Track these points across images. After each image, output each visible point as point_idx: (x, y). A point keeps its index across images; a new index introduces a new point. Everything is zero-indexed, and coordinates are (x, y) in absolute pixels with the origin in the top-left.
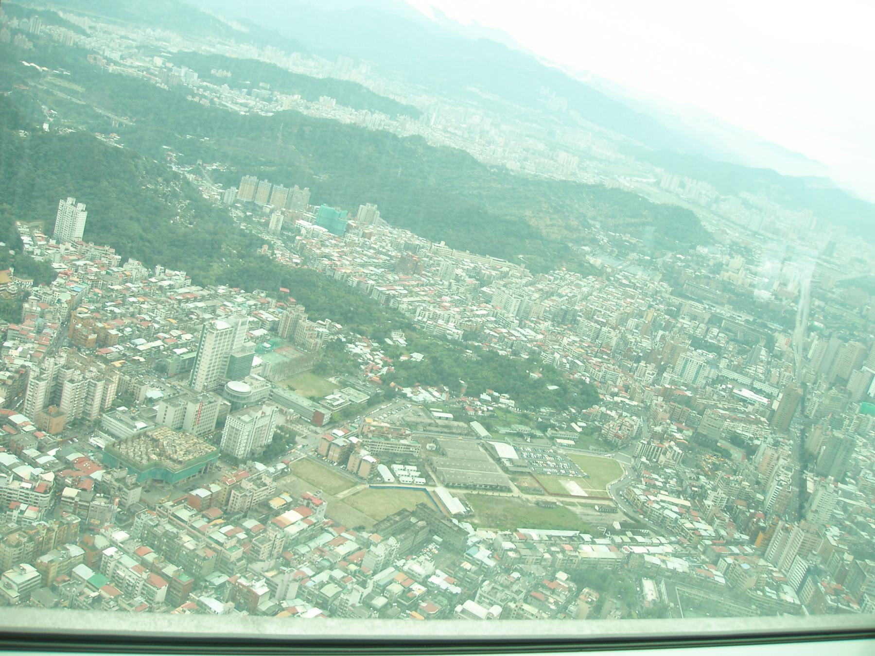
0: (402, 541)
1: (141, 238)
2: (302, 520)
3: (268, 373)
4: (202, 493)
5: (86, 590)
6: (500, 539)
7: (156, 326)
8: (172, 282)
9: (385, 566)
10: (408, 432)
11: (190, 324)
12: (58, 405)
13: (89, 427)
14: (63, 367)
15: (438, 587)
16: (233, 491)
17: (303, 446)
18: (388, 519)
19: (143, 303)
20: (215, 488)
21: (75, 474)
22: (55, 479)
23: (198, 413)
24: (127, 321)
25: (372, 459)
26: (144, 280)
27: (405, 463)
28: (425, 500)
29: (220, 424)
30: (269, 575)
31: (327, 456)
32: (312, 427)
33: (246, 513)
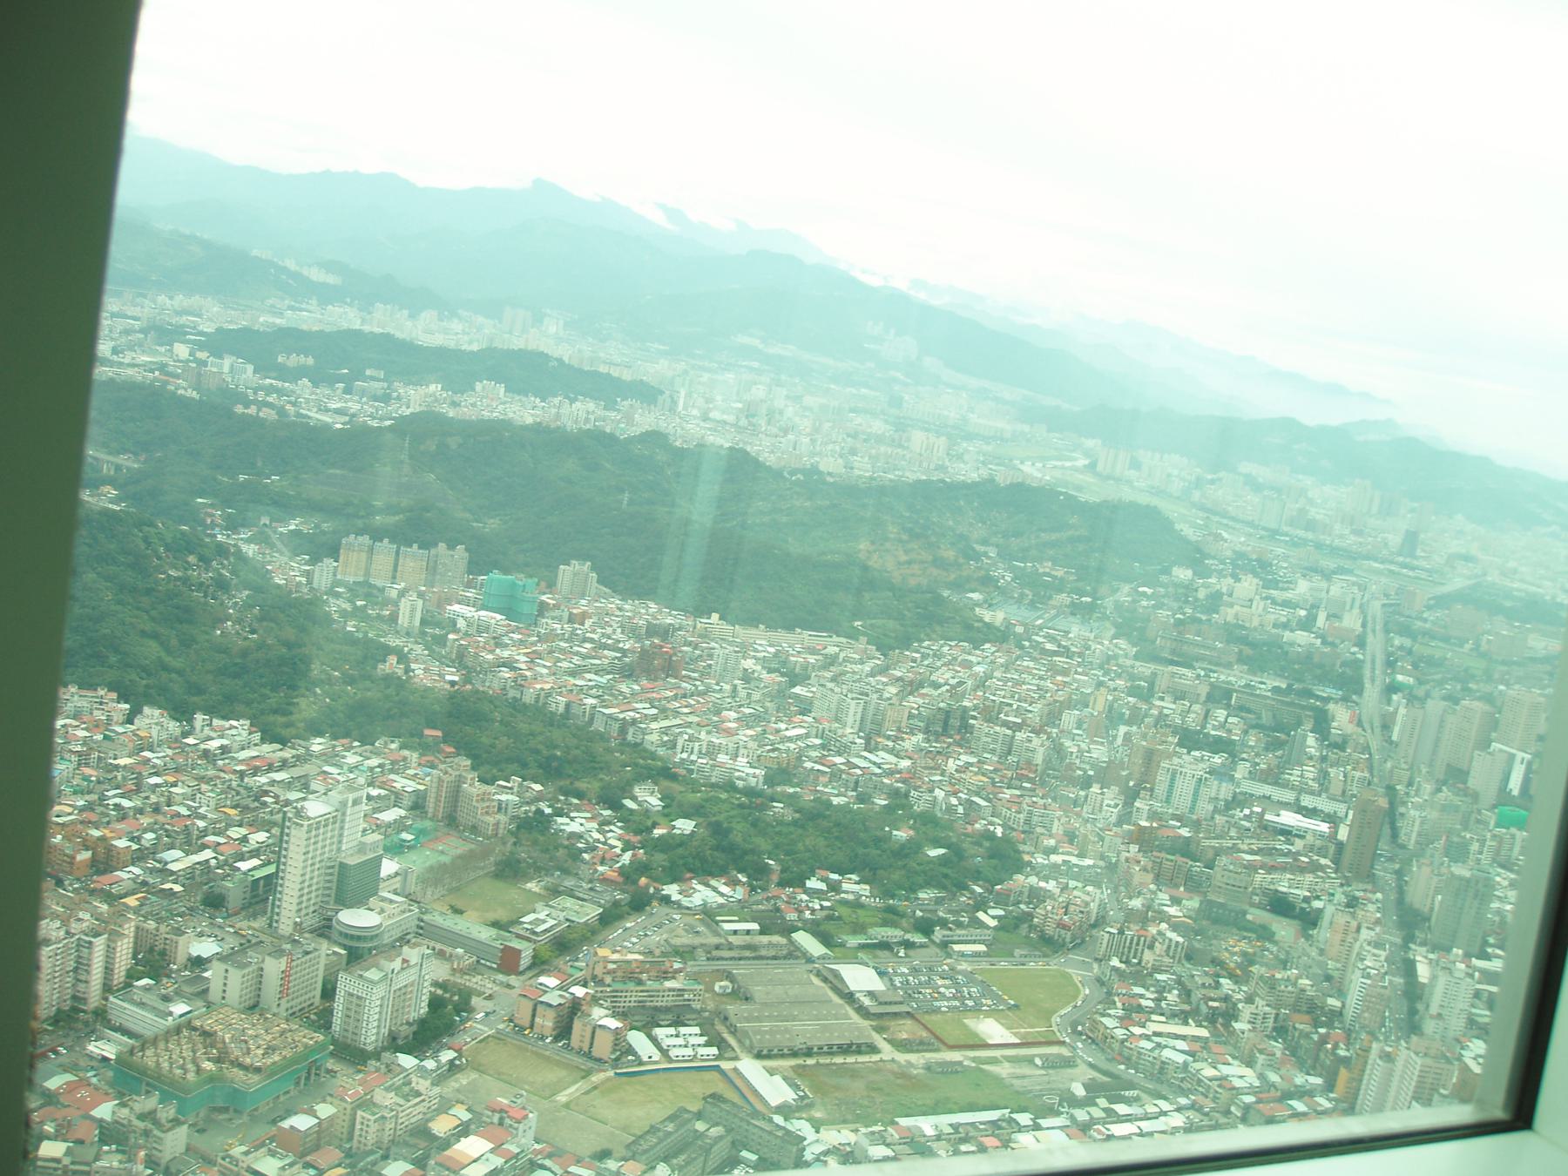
0: (681, 1168)
1: (165, 668)
2: (492, 1151)
3: (412, 887)
4: (302, 1122)
6: (865, 1142)
7: (201, 824)
8: (225, 742)
10: (677, 966)
11: (264, 815)
13: (86, 1023)
16: (359, 1113)
17: (487, 1014)
18: (653, 1130)
19: (174, 785)
20: (325, 1110)
21: (60, 1114)
23: (286, 975)
24: (145, 821)
25: (613, 1023)
26: (175, 742)
27: (678, 1023)
28: (721, 1087)
29: (328, 993)
31: (532, 1027)
32: (501, 977)
33: (388, 1149)
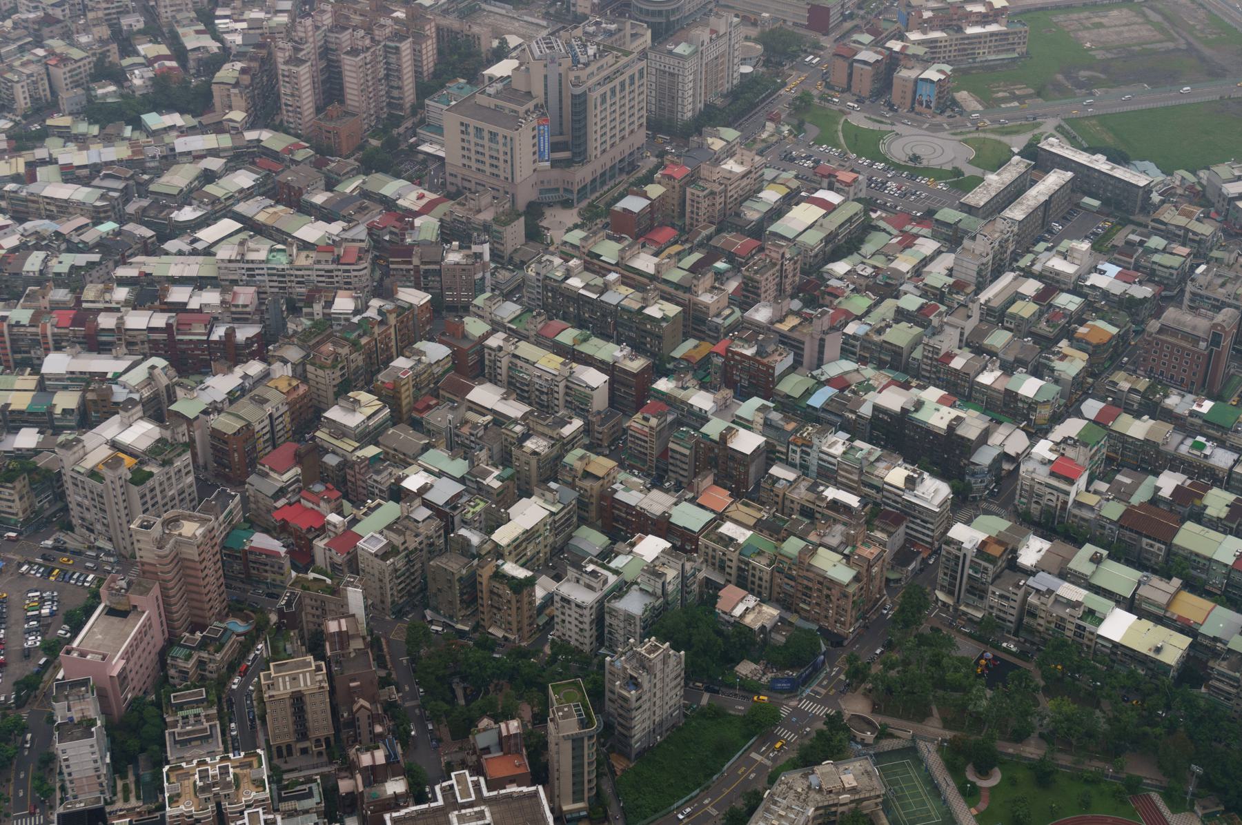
4: (634, 204)
5: (471, 416)
9: (997, 274)
12: (342, 101)
14: (331, 31)
15: (1105, 294)
22: (370, 234)
30: (785, 327)
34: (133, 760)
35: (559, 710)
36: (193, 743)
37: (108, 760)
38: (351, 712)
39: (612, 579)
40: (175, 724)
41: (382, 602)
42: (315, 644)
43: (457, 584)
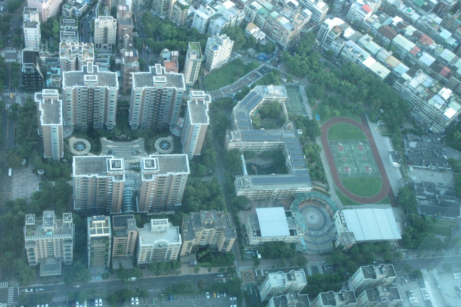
34: (48, 38)
35: (191, 51)
36: (69, 37)
37: (40, 37)
38: (122, 37)
39: (214, 12)
40: (63, 29)
41: (137, 3)
42: (114, 12)
43: (163, 3)
